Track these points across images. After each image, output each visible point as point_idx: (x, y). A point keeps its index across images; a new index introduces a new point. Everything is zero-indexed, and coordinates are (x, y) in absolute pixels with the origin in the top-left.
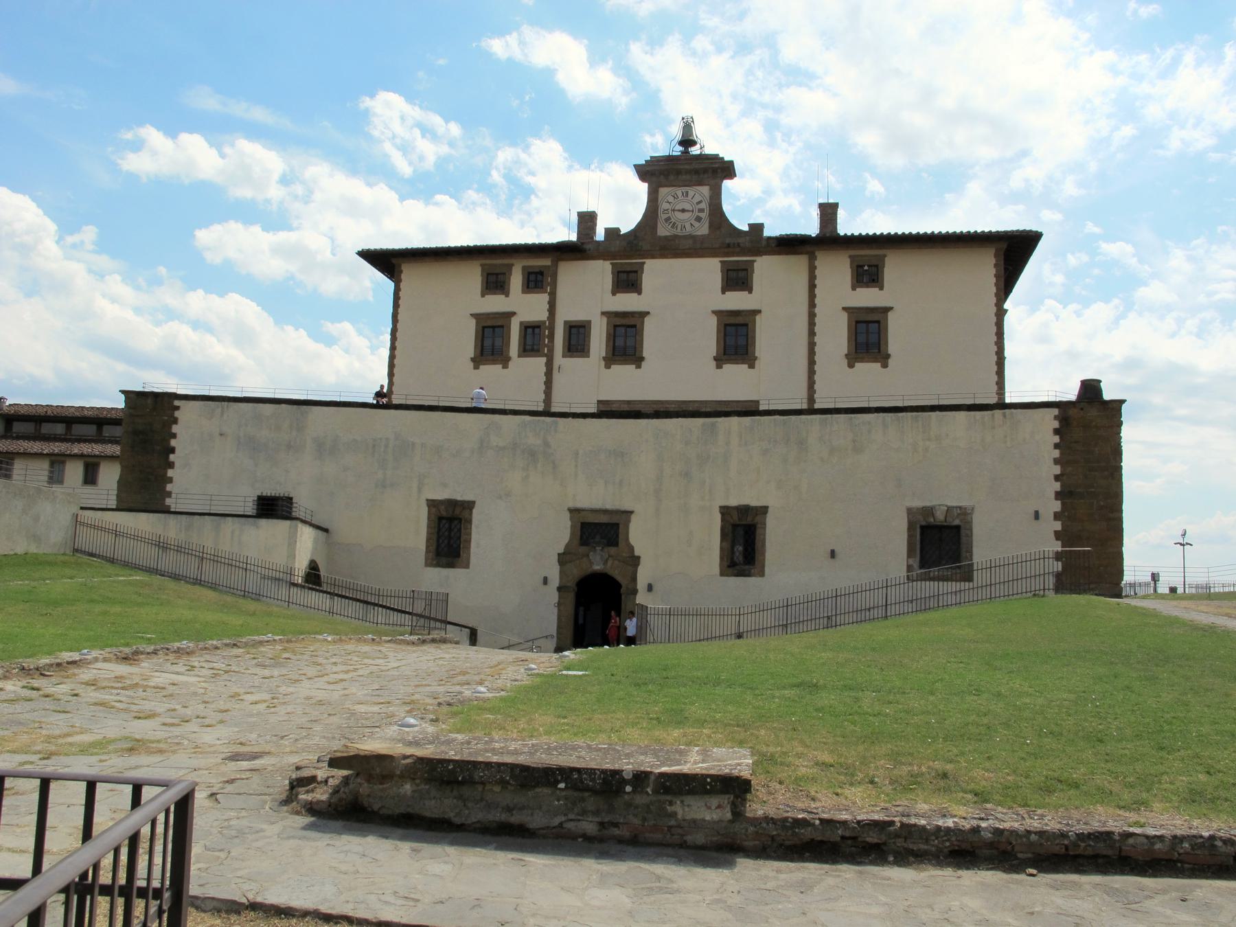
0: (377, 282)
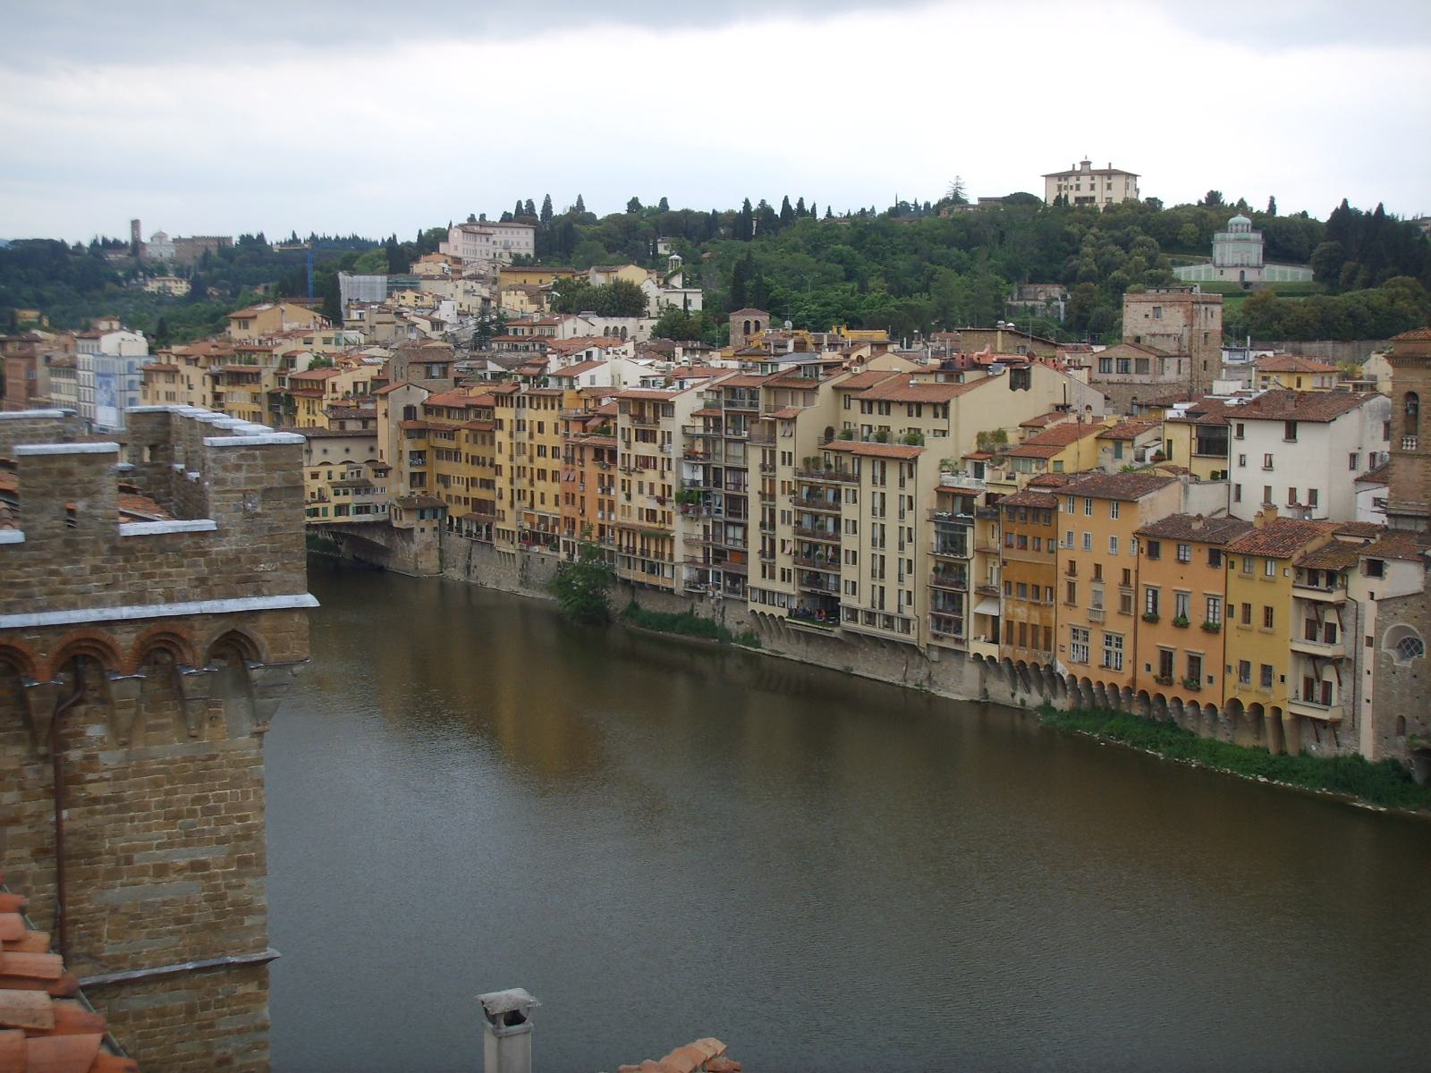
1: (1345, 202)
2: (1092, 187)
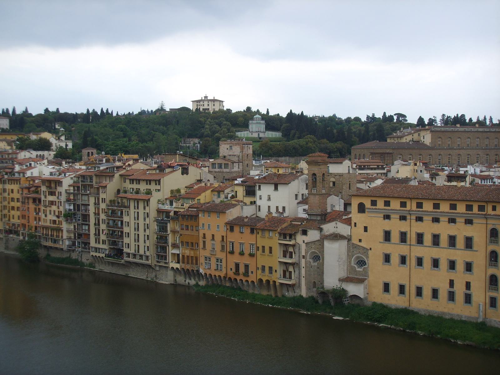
0: (192, 102)
1: (291, 111)
2: (208, 105)
